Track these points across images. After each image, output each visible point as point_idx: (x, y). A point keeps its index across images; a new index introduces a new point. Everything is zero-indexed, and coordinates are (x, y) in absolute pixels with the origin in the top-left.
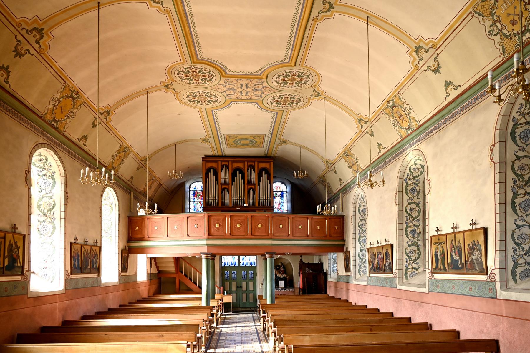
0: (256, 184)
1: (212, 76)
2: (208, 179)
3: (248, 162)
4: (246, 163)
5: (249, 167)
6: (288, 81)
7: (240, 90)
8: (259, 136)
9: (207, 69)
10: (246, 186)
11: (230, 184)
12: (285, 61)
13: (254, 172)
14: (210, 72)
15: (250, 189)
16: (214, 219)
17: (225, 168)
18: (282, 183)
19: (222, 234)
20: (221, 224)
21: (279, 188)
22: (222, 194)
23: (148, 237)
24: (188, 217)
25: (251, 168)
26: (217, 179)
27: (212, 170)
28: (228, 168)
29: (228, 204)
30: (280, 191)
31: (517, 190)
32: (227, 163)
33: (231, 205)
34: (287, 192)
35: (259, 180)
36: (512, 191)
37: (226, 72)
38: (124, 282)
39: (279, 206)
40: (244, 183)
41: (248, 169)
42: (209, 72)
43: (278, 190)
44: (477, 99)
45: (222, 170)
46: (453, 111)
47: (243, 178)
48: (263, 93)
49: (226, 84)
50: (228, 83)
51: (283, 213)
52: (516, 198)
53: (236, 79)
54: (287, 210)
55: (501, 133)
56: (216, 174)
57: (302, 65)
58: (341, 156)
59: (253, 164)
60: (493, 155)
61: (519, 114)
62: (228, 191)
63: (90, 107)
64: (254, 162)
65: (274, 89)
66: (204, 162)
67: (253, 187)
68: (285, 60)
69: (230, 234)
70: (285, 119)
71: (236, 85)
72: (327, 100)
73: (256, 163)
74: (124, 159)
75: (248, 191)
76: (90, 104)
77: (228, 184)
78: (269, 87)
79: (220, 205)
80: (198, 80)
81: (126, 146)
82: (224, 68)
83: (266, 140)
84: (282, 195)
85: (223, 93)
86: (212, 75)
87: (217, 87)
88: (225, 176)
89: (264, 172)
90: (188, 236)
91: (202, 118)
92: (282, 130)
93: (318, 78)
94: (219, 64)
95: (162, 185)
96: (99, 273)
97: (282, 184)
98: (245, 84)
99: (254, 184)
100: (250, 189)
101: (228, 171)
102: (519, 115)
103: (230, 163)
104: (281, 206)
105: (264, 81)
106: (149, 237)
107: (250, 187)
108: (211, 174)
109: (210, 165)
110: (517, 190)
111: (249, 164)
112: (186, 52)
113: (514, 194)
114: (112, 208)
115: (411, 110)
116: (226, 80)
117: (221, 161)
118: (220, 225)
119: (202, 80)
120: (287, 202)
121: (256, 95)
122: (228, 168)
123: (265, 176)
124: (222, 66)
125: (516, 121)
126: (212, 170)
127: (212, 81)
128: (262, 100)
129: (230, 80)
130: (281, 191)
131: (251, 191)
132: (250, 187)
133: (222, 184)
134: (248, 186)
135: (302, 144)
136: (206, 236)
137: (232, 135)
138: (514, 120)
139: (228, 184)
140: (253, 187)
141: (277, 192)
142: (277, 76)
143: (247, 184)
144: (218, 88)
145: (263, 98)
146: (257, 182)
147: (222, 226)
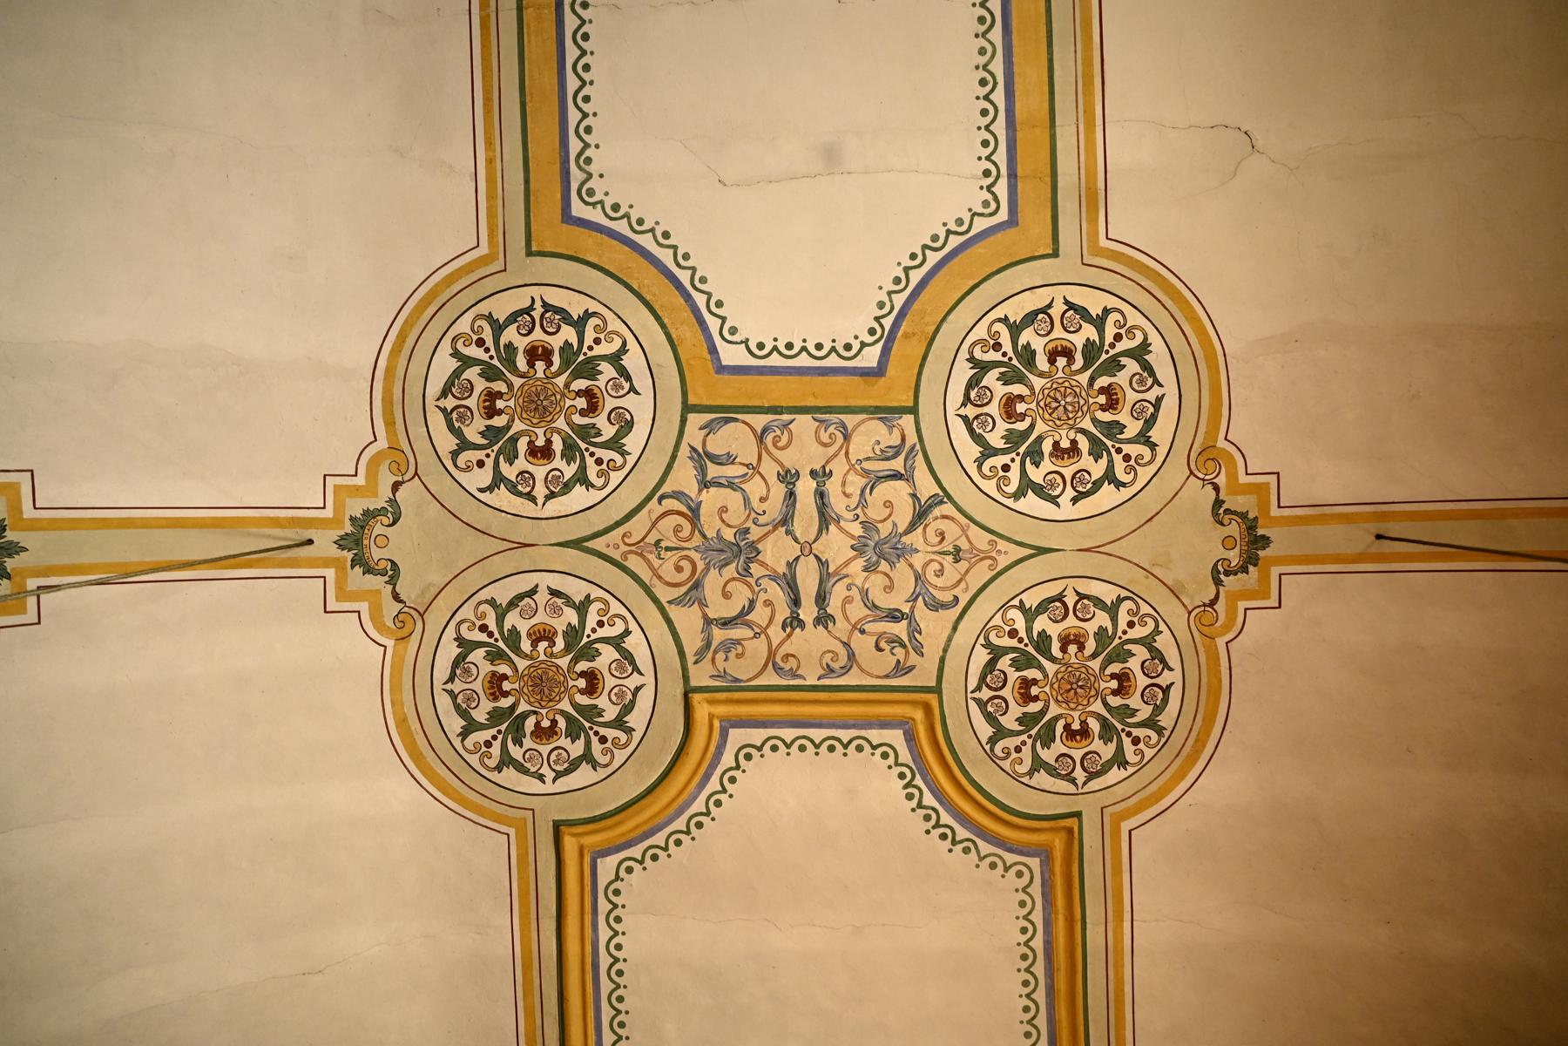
1: (985, 694)
6: (564, 662)
7: (836, 546)
9: (1006, 764)
12: (613, 860)
14: (993, 741)
37: (911, 738)
42: (1000, 733)
48: (694, 514)
49: (910, 617)
50: (900, 629)
53: (851, 679)
57: (520, 826)
65: (633, 563)
68: (617, 878)
71: (858, 611)
78: (664, 594)
80: (1065, 642)
82: (919, 781)
85: (936, 501)
86: (982, 704)
87: (963, 565)
91: (1093, 76)
93: (405, 720)
94: (946, 818)
98: (801, 624)
105: (700, 656)
112: (1094, 912)
116: (914, 658)
119: (1043, 642)
121: (731, 485)
124: (929, 800)
127: (988, 645)
128: (687, 408)
129: (887, 661)
142: (636, 720)
144: (957, 554)
145: (684, 451)
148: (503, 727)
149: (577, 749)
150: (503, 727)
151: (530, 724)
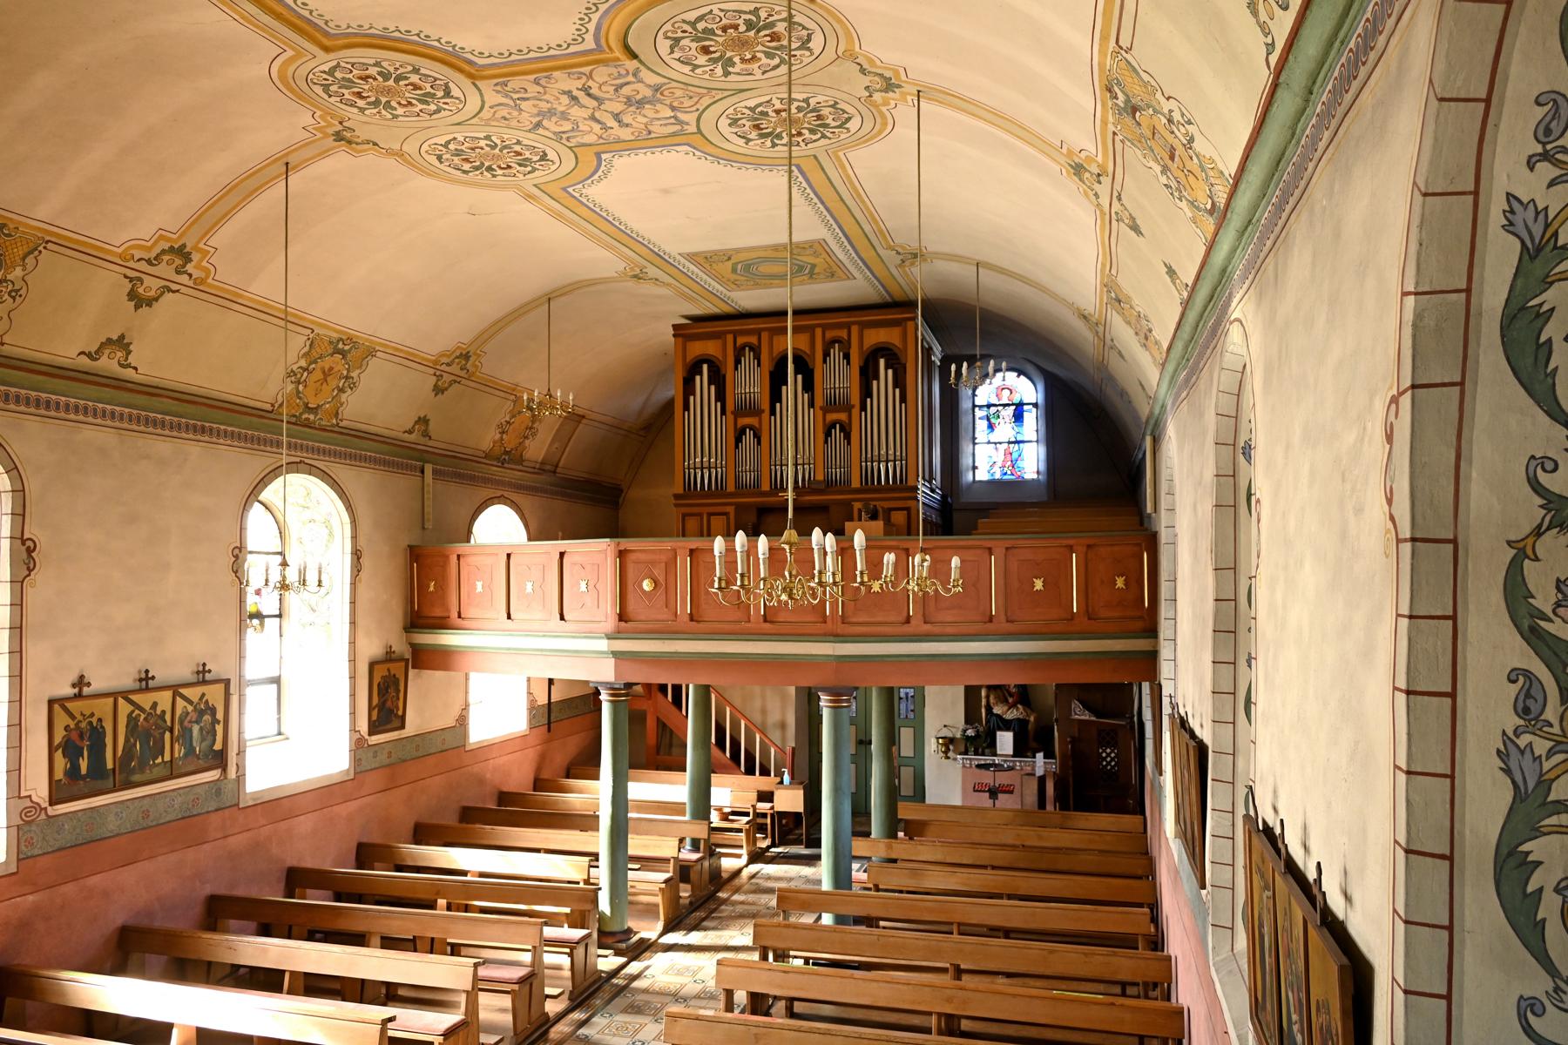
0: (853, 406)
2: (692, 398)
3: (825, 328)
4: (819, 331)
5: (828, 346)
8: (806, 246)
10: (820, 413)
11: (763, 411)
13: (848, 363)
15: (833, 426)
16: (637, 562)
17: (748, 356)
18: (1020, 373)
19: (664, 617)
20: (661, 579)
21: (1006, 392)
22: (737, 447)
23: (459, 617)
24: (562, 555)
25: (836, 352)
26: (721, 397)
27: (705, 367)
28: (758, 357)
29: (757, 484)
30: (1013, 404)
31: (1547, 766)
32: (753, 340)
33: (766, 487)
34: (1035, 405)
35: (866, 392)
36: (1507, 771)
38: (387, 761)
39: (1008, 458)
40: (812, 404)
41: (826, 354)
43: (1005, 401)
44: (1367, 45)
45: (738, 362)
46: (1304, 131)
47: (808, 386)
51: (1020, 484)
52: (1536, 833)
54: (1038, 472)
55: (1430, 322)
56: (717, 379)
58: (1105, 301)
59: (843, 334)
60: (1392, 473)
61: (1546, 171)
62: (757, 437)
63: (88, 253)
64: (848, 326)
66: (680, 339)
67: (843, 416)
69: (691, 614)
70: (847, 181)
72: (925, 98)
73: (855, 330)
74: (354, 374)
75: (828, 434)
76: (77, 242)
77: (755, 411)
79: (731, 488)
81: (335, 335)
83: (841, 256)
84: (1018, 417)
88: (749, 382)
89: (882, 362)
90: (562, 618)
92: (873, 220)
95: (583, 417)
96: (226, 765)
97: (1018, 376)
99: (848, 408)
100: (833, 426)
101: (759, 365)
102: (1552, 184)
103: (765, 336)
104: (1015, 456)
106: (463, 616)
107: (832, 417)
108: (702, 381)
109: (698, 349)
110: (1547, 766)
111: (830, 334)
113: (1519, 796)
114: (331, 534)
115: (1189, 123)
117: (736, 334)
118: (656, 582)
120: (1037, 441)
122: (758, 357)
123: (885, 375)
125: (1537, 230)
126: (705, 367)
130: (1016, 401)
131: (837, 433)
132: (832, 417)
133: (738, 413)
134: (824, 419)
135: (979, 258)
136: (610, 623)
137: (713, 251)
138: (1518, 219)
139: (757, 412)
140: (843, 416)
141: (1000, 408)
143: (821, 408)
146: (855, 400)
147: (665, 586)
148: (761, 23)
149: (701, 26)
150: (761, 23)
151: (742, 28)
